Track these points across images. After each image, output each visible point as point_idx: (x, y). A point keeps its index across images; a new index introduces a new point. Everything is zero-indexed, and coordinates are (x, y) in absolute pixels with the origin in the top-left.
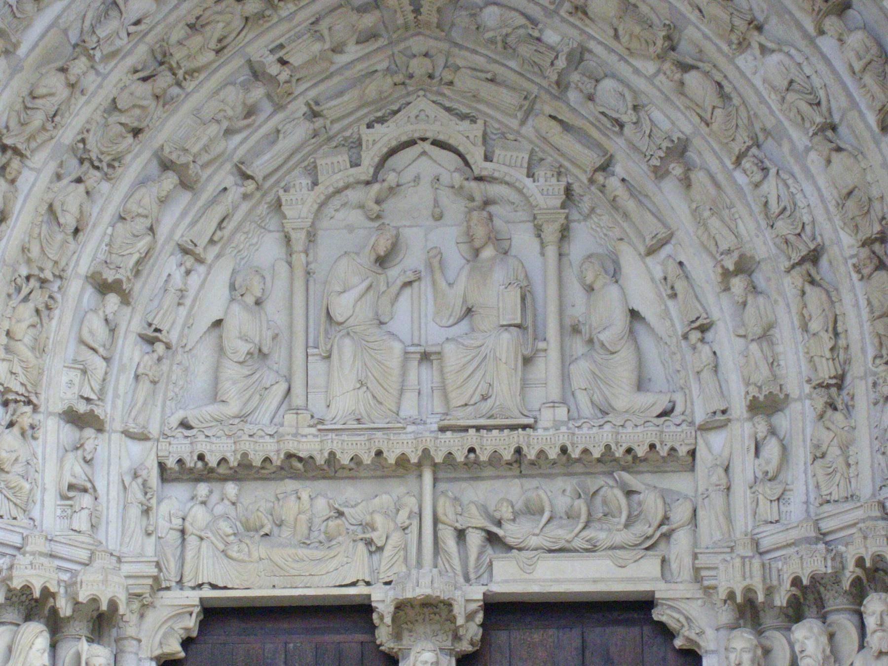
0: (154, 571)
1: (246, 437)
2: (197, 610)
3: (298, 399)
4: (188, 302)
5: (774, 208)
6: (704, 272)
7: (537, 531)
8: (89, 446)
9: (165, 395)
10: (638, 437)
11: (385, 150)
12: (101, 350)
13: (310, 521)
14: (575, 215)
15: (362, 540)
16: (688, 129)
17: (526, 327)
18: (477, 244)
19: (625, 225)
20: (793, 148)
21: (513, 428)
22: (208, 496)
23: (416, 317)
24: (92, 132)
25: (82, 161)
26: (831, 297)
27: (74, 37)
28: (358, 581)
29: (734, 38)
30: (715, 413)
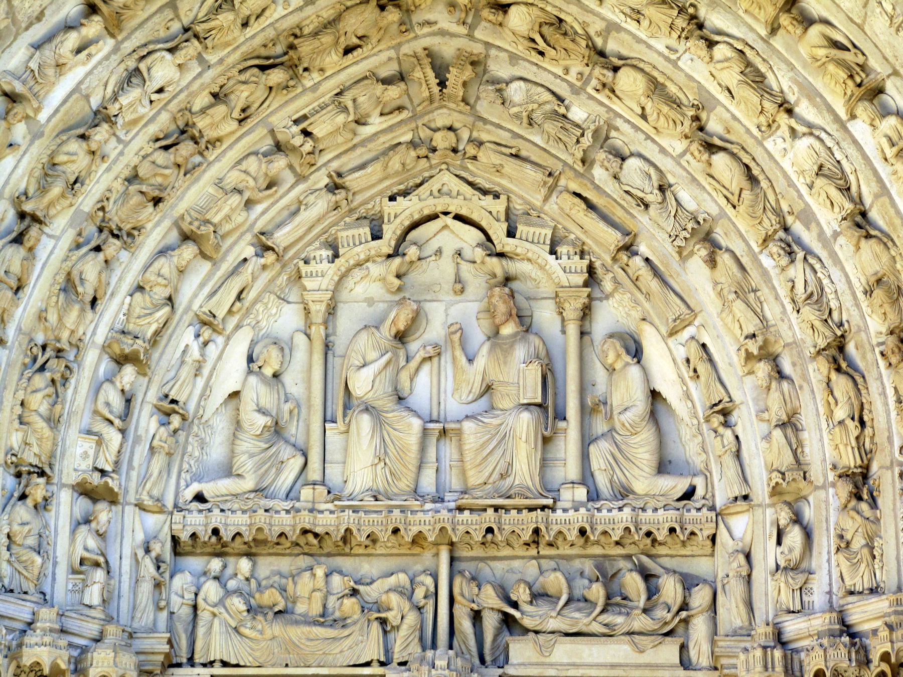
1: (261, 512)
3: (314, 473)
4: (206, 372)
6: (727, 354)
7: (554, 614)
8: (103, 517)
9: (181, 466)
11: (407, 223)
12: (117, 422)
15: (377, 619)
16: (714, 211)
17: (548, 409)
19: (647, 305)
20: (821, 235)
21: (531, 509)
22: (222, 571)
24: (112, 201)
25: (101, 230)
27: (95, 102)
28: (372, 661)
29: (763, 120)
30: (736, 498)
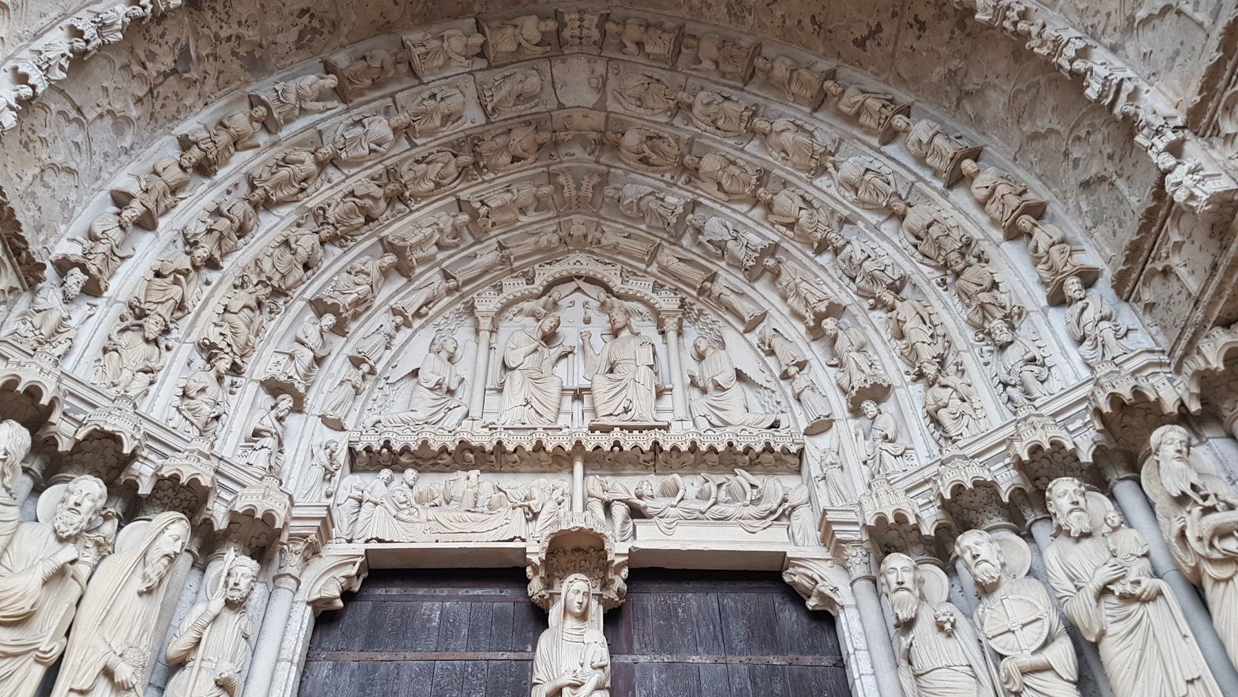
0: (324, 513)
2: (360, 560)
3: (475, 413)
4: (394, 349)
5: (859, 256)
6: (796, 331)
13: (476, 495)
14: (685, 322)
16: (777, 239)
18: (618, 325)
19: (728, 317)
23: (574, 373)
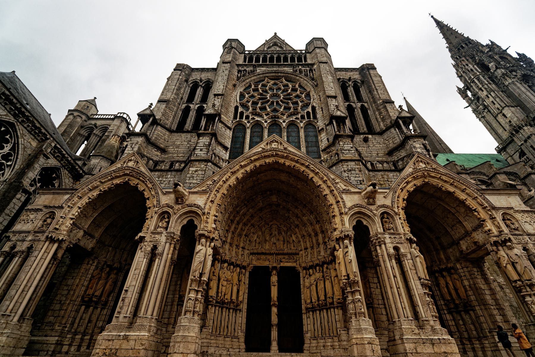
6: (300, 236)
10: (294, 251)
17: (284, 241)
23: (273, 240)
26: (312, 238)
